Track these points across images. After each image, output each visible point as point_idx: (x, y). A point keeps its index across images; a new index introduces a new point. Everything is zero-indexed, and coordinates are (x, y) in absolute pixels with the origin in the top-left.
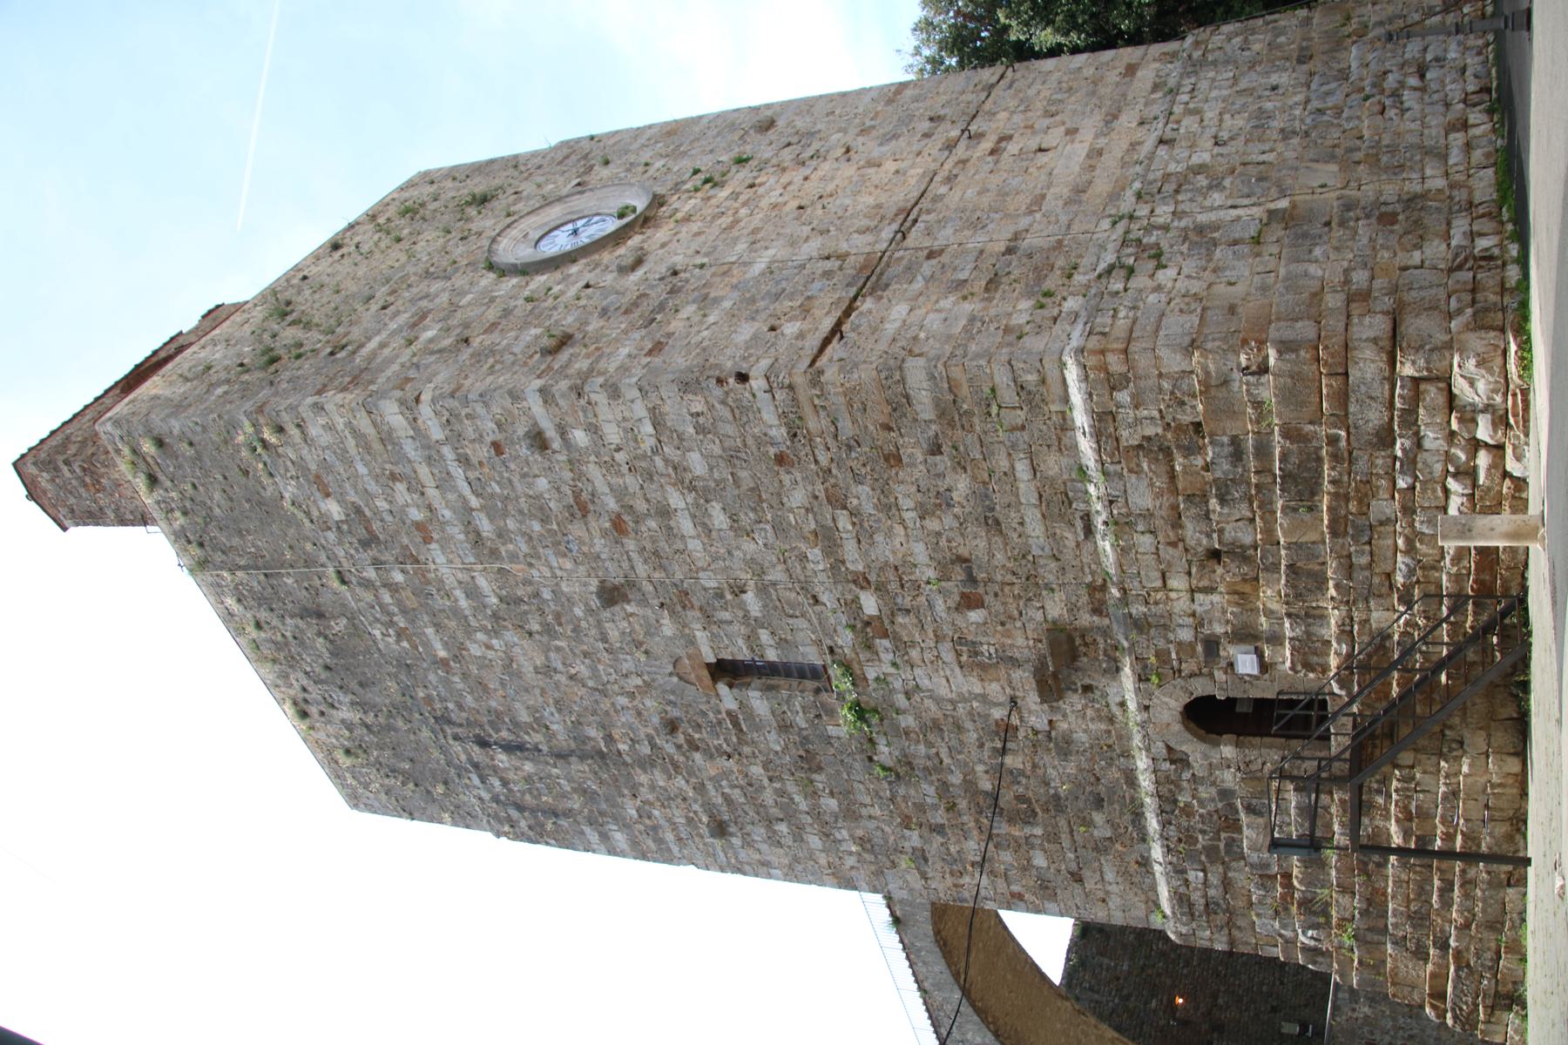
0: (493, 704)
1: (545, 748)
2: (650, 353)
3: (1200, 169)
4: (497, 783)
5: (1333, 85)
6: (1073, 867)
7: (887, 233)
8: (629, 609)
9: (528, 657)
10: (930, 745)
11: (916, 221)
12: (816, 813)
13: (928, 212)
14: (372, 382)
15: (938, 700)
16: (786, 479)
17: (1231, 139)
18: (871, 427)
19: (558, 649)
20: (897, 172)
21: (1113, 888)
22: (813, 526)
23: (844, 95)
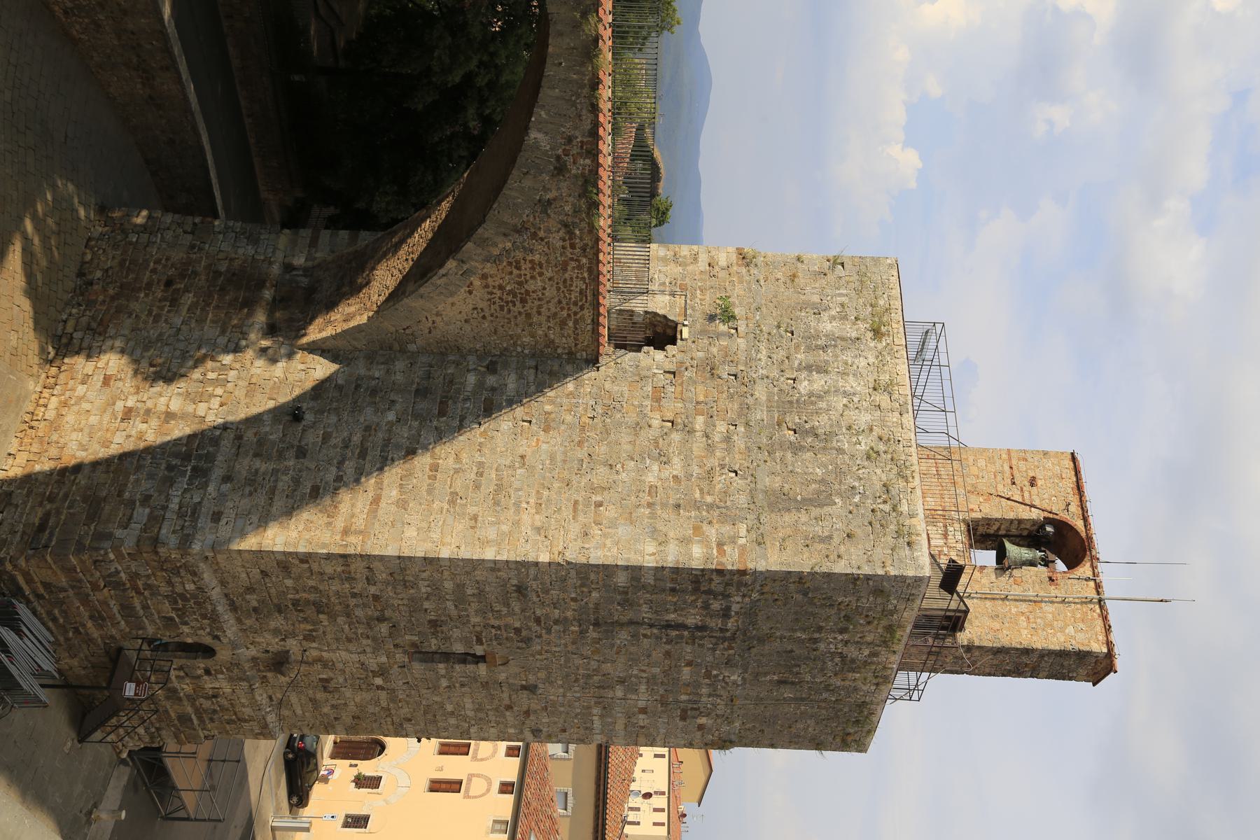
6: (267, 580)
15: (347, 650)
21: (240, 570)
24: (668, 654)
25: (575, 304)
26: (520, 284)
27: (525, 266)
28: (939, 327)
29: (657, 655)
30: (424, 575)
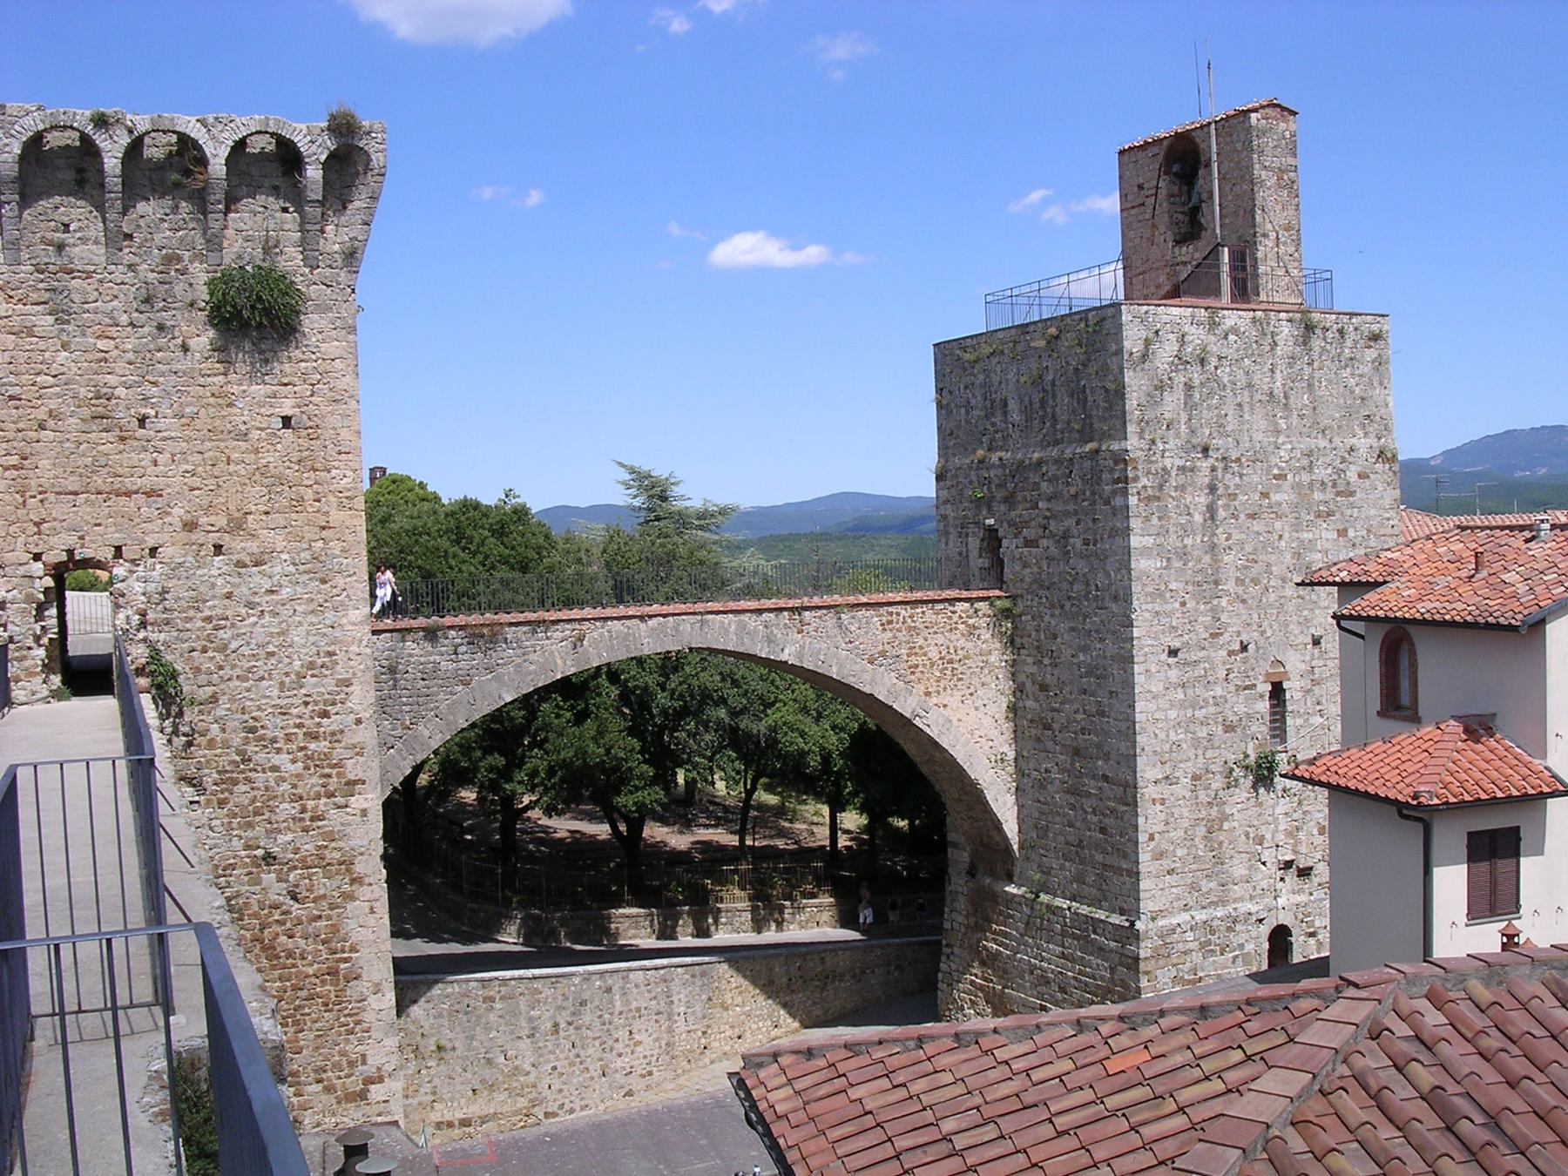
15: (1273, 807)
24: (1252, 516)
25: (950, 618)
26: (932, 665)
27: (913, 660)
28: (989, 299)
29: (1257, 526)
30: (1162, 735)
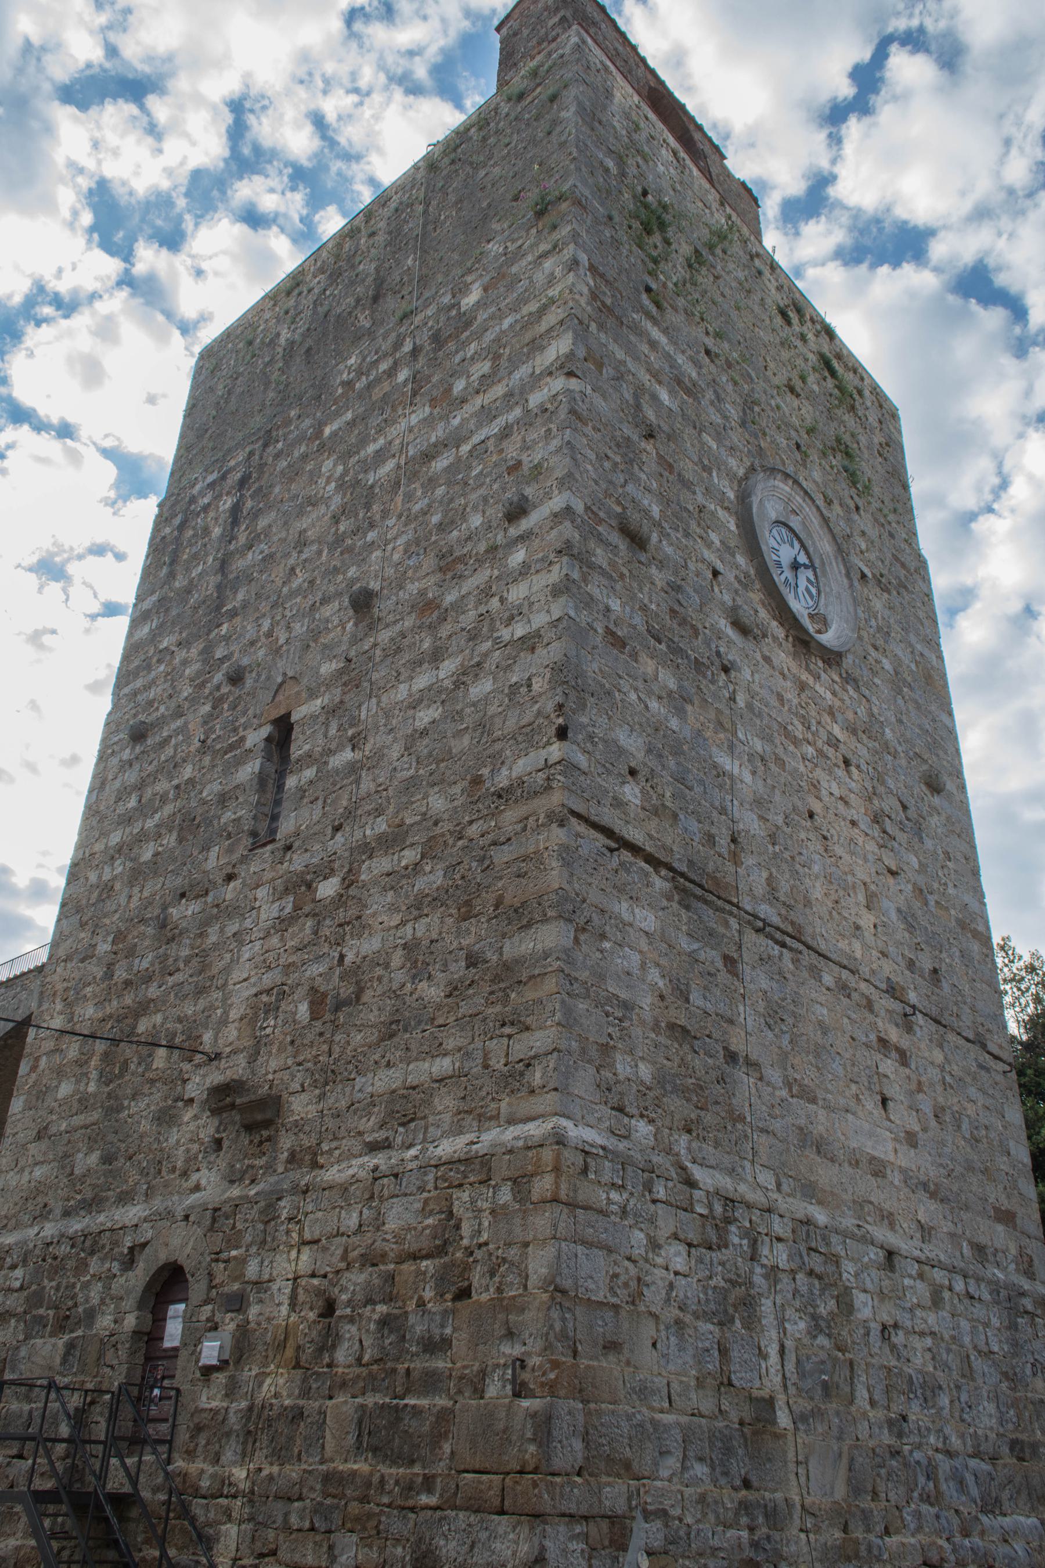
0: (277, 490)
1: (232, 547)
2: (609, 632)
3: (846, 1305)
4: (206, 500)
5: (975, 1492)
6: (53, 1130)
7: (765, 910)
8: (350, 625)
9: (313, 523)
10: (187, 961)
11: (783, 945)
12: (142, 838)
13: (795, 961)
14: (601, 326)
15: (227, 970)
16: (457, 789)
17: (893, 1348)
18: (500, 885)
19: (319, 553)
20: (858, 928)
22: (408, 821)
23: (976, 873)
